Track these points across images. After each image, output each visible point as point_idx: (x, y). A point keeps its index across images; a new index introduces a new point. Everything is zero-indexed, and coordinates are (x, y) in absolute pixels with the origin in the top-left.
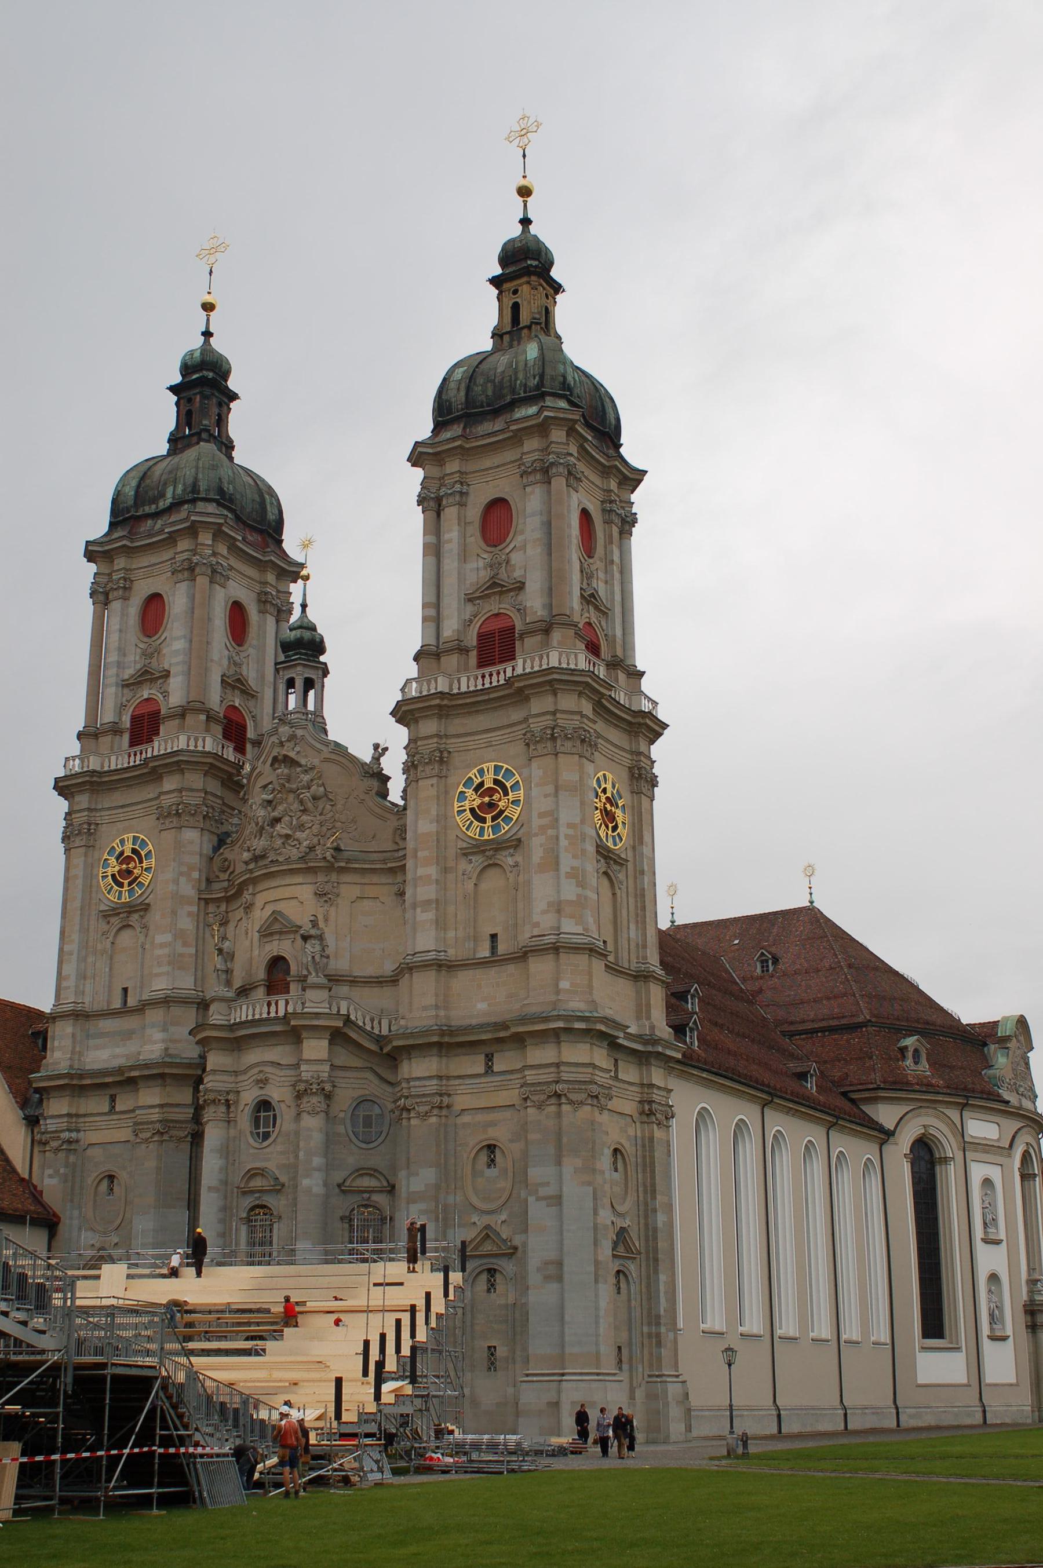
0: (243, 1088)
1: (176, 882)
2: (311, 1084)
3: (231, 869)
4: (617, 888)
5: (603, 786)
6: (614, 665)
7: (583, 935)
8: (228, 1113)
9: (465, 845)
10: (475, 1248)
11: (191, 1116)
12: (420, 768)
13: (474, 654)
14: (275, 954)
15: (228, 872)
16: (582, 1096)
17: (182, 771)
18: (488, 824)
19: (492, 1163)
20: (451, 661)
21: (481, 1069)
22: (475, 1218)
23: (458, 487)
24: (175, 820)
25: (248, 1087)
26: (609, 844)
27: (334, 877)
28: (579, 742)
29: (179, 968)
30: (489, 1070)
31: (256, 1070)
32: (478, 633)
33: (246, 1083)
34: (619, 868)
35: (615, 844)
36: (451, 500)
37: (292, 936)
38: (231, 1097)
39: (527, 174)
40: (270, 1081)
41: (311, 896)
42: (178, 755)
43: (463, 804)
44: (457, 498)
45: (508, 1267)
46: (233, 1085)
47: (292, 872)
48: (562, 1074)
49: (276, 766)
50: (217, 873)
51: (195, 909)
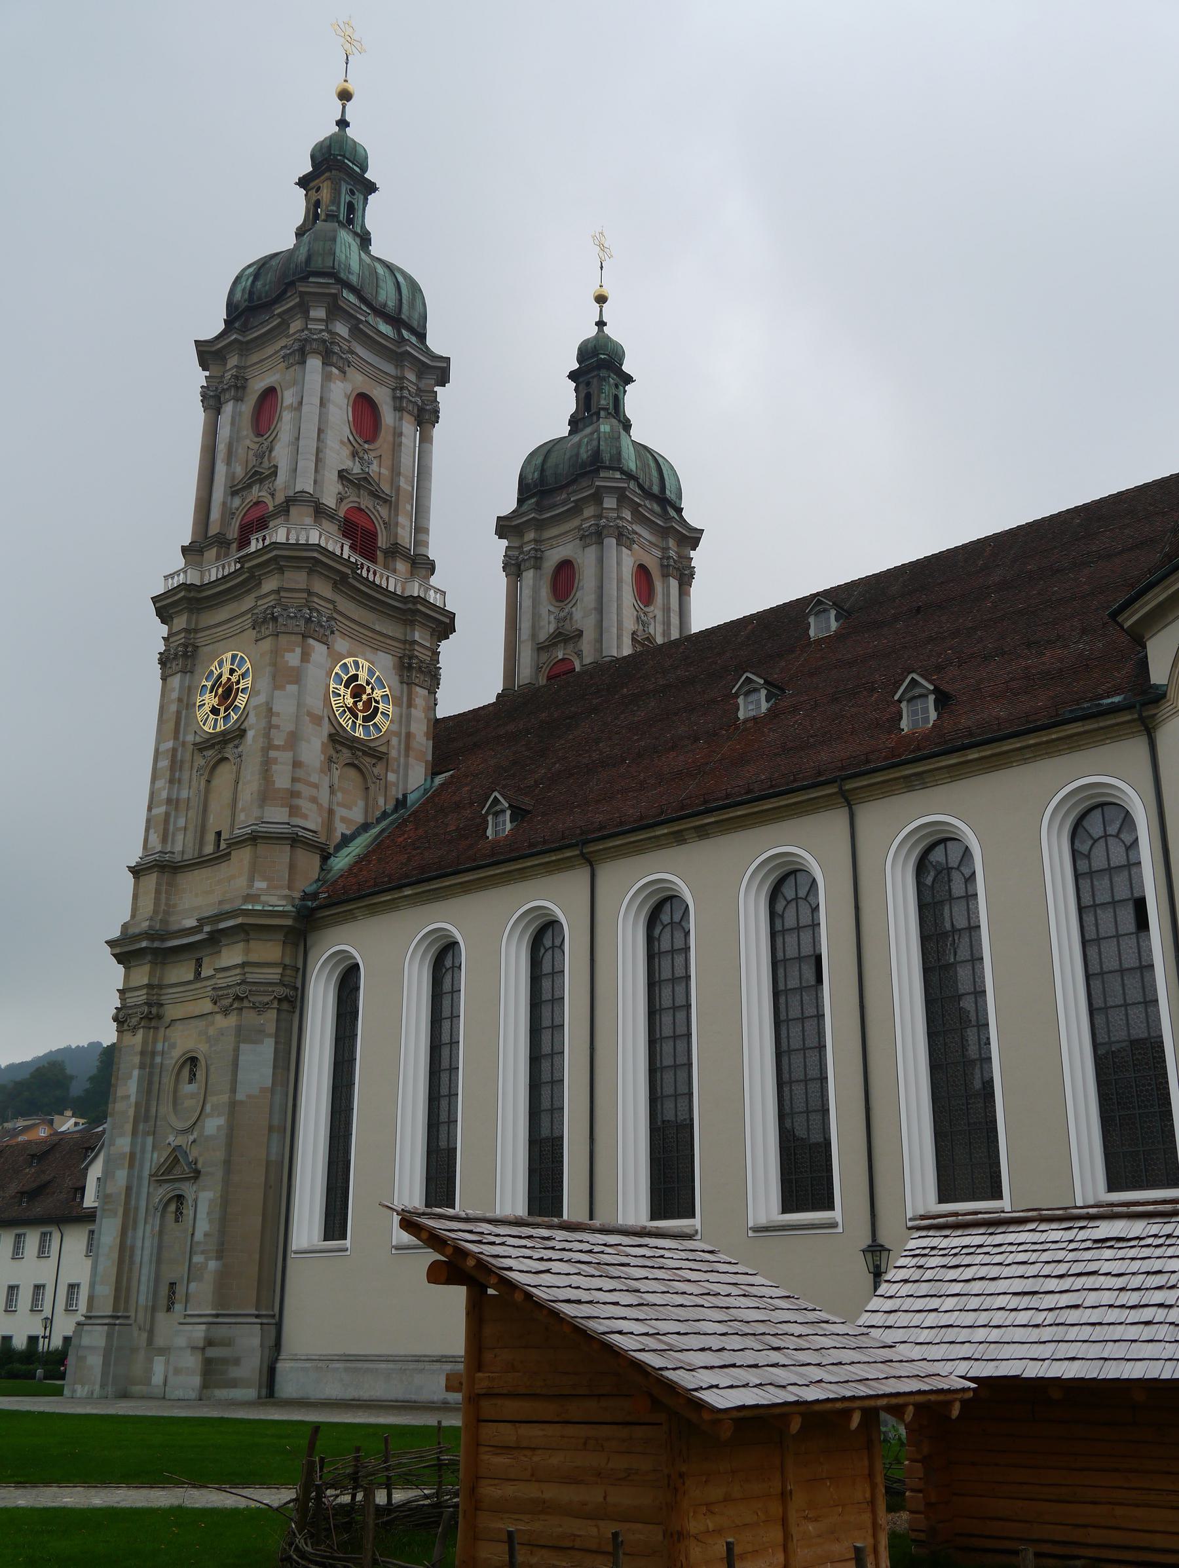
4: (369, 781)
5: (352, 672)
6: (393, 553)
7: (288, 824)
9: (201, 740)
10: (169, 1171)
12: (169, 665)
13: (234, 546)
16: (266, 999)
18: (221, 716)
19: (192, 1077)
20: (211, 553)
21: (191, 977)
22: (171, 1139)
26: (357, 735)
28: (302, 622)
30: (198, 974)
32: (240, 525)
34: (374, 761)
35: (367, 733)
39: (348, 78)
43: (203, 698)
45: (188, 1190)
48: (247, 975)
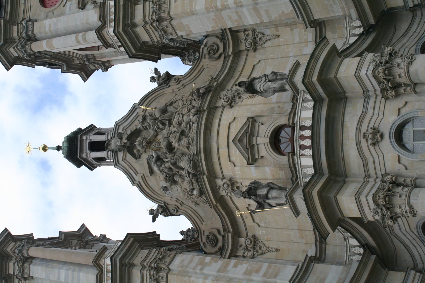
0: (382, 167)
1: (206, 277)
2: (381, 63)
3: (216, 233)
8: (406, 186)
11: (418, 274)
14: (267, 140)
15: (218, 236)
17: (132, 265)
23: (24, 23)
24: (162, 274)
25: (381, 158)
27: (223, 94)
29: (275, 277)
31: (363, 141)
33: (376, 161)
36: (30, 28)
37: (257, 125)
38: (388, 178)
40: (376, 126)
41: (232, 110)
42: (115, 261)
44: (30, 23)
46: (379, 181)
47: (208, 128)
49: (135, 151)
50: (217, 249)
51: (233, 261)
